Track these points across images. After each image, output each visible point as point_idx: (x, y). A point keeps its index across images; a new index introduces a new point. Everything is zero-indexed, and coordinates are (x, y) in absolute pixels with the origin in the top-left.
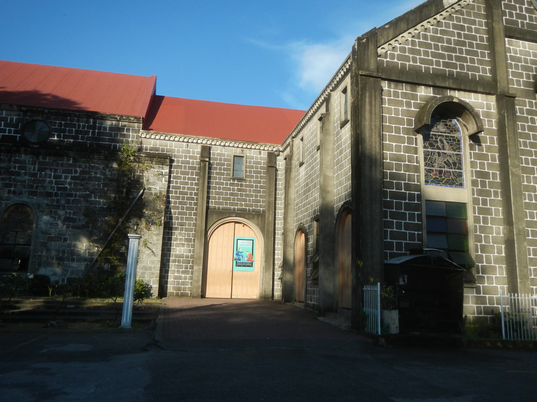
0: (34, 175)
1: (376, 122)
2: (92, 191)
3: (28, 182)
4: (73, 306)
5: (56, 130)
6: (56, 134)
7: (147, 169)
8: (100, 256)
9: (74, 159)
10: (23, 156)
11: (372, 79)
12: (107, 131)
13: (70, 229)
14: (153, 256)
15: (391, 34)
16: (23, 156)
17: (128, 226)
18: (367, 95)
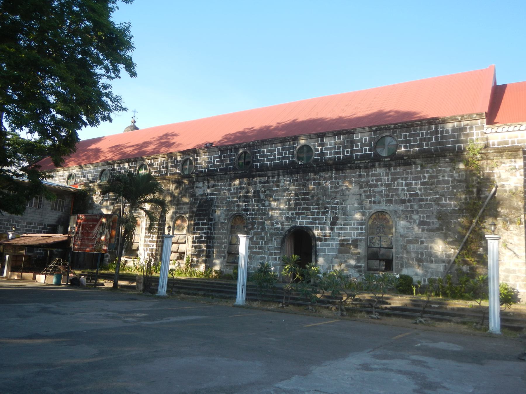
0: (389, 185)
2: (442, 194)
3: (385, 192)
4: (437, 306)
5: (402, 142)
6: (403, 145)
7: (497, 165)
8: (457, 257)
9: (422, 166)
10: (378, 169)
12: (450, 134)
13: (425, 232)
14: (516, 258)
16: (378, 169)
17: (483, 226)
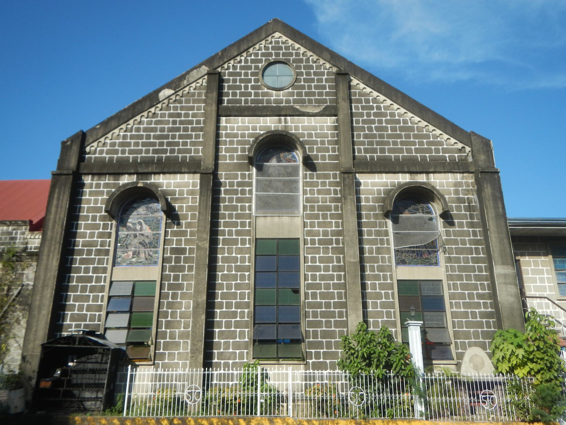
1: (60, 214)
11: (63, 177)
15: (100, 133)
18: (57, 191)
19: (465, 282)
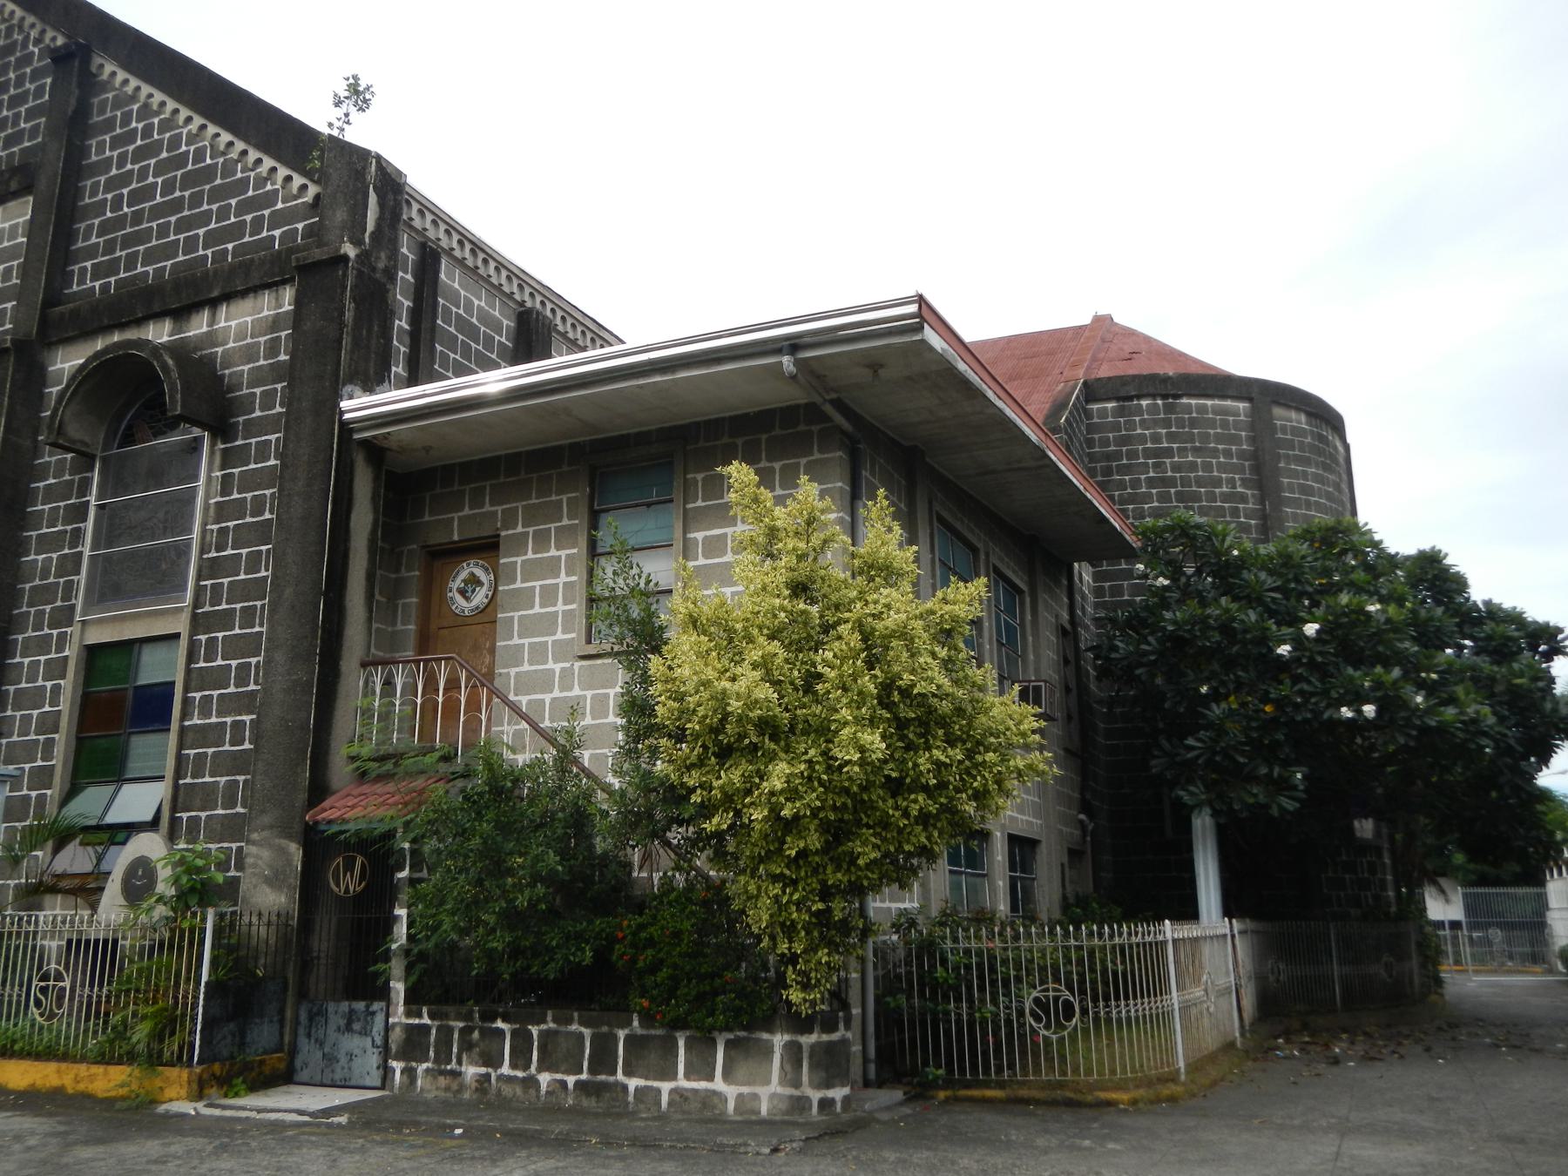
19: (237, 631)
